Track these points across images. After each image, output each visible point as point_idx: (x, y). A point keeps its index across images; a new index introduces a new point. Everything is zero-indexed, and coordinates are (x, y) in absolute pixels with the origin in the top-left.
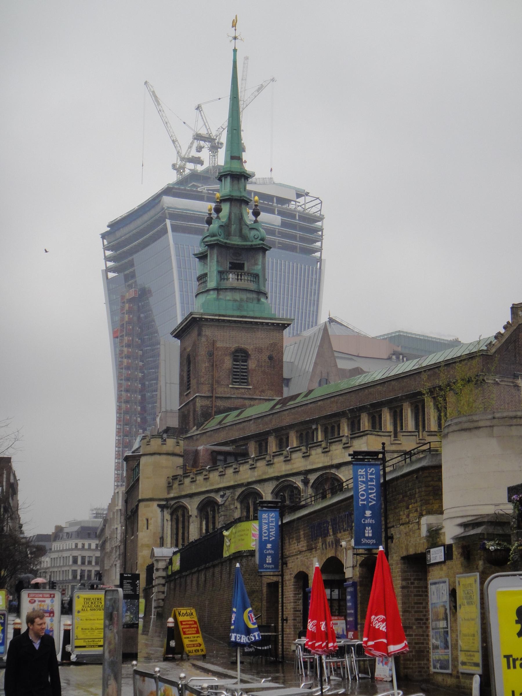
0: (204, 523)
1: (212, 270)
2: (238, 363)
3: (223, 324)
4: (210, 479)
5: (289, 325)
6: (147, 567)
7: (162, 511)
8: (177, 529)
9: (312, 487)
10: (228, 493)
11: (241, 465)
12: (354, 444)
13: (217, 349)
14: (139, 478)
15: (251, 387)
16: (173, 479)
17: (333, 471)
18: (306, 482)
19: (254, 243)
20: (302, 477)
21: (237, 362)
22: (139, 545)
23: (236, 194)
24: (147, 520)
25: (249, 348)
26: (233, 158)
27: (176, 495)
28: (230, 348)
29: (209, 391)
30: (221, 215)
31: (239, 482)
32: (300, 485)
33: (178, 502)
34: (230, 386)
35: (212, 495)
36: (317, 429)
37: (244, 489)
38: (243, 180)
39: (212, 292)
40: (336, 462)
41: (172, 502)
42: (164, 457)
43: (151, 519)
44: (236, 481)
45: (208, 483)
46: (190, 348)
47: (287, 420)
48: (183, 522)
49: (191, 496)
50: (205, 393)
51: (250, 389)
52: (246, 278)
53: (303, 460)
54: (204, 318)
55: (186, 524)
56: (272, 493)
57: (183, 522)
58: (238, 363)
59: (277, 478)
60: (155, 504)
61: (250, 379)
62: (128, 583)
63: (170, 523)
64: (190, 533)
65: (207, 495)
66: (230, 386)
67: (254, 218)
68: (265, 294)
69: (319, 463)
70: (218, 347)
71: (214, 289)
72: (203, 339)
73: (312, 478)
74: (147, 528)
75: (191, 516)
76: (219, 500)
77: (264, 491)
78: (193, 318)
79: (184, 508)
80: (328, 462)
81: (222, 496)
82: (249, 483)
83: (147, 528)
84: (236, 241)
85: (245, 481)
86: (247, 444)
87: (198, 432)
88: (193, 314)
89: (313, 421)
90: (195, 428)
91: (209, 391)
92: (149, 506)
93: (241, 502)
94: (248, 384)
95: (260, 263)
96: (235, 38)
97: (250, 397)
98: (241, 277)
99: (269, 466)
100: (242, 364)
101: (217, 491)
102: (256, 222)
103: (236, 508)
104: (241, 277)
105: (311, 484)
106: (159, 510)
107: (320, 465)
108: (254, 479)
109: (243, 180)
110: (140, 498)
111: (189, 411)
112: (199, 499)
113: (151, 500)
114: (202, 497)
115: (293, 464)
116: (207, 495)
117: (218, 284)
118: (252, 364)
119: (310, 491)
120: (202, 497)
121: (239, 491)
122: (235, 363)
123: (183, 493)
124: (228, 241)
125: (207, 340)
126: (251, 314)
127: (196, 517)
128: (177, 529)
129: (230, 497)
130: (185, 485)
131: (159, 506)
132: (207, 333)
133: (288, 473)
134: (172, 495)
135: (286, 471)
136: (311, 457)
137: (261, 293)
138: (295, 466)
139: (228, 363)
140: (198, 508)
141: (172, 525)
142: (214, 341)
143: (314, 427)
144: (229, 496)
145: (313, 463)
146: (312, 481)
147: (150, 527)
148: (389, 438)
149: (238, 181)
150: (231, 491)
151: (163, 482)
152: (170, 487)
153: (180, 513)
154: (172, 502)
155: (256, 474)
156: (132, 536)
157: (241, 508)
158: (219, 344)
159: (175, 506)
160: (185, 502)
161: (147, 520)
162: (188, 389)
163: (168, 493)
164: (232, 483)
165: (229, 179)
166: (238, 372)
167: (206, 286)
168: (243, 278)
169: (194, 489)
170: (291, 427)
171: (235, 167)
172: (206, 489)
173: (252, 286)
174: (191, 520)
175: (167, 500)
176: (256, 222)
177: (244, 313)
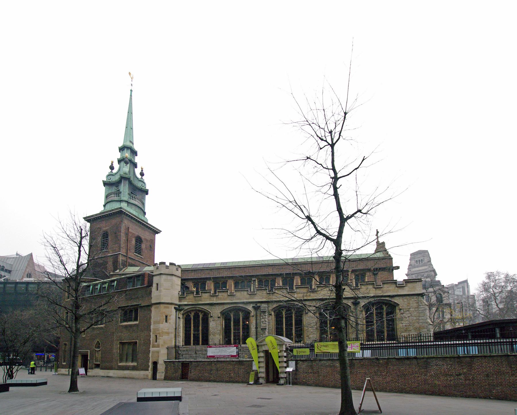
0: (224, 321)
10: (264, 305)
12: (408, 285)
18: (356, 304)
20: (352, 301)
24: (166, 317)
41: (186, 308)
43: (170, 316)
45: (235, 298)
50: (123, 253)
60: (173, 306)
63: (182, 320)
65: (235, 305)
74: (166, 321)
78: (121, 210)
83: (166, 321)
88: (122, 208)
92: (168, 308)
106: (174, 311)
112: (222, 307)
113: (171, 304)
116: (235, 305)
121: (275, 305)
131: (175, 308)
136: (361, 290)
141: (183, 321)
147: (169, 321)
153: (192, 315)
154: (186, 308)
155: (296, 296)
161: (166, 317)
168: (136, 200)
173: (141, 206)
175: (179, 306)
176: (142, 178)
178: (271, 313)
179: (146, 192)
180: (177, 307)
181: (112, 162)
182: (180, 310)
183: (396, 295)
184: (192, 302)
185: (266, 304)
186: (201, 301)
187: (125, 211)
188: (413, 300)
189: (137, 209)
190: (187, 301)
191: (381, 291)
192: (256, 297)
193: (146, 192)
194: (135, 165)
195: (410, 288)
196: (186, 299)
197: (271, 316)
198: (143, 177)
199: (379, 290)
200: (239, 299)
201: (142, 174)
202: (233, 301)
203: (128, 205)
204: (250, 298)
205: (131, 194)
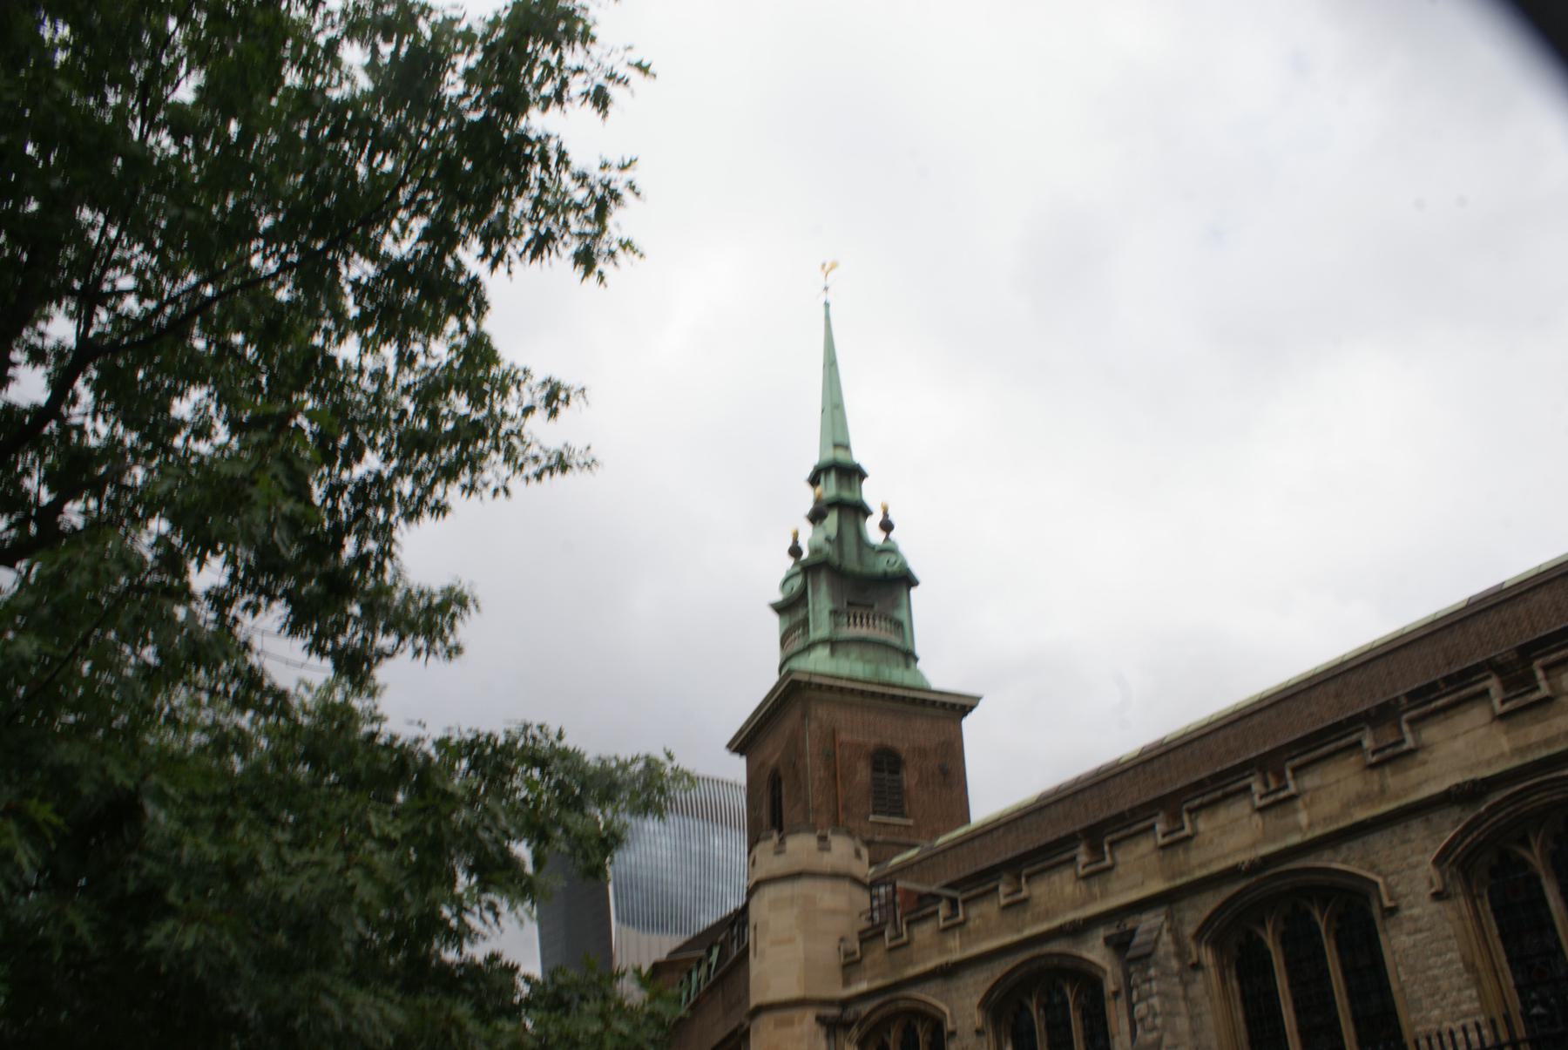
5: (972, 708)
10: (1149, 921)
15: (910, 822)
16: (862, 941)
23: (846, 495)
25: (902, 747)
26: (836, 446)
27: (878, 983)
31: (1199, 873)
33: (891, 1001)
34: (872, 818)
37: (1229, 891)
38: (857, 478)
41: (865, 1008)
42: (828, 884)
44: (1182, 874)
45: (1028, 916)
46: (777, 755)
49: (948, 972)
51: (907, 827)
56: (1438, 861)
60: (810, 1015)
66: (872, 818)
67: (882, 536)
68: (916, 659)
71: (823, 642)
72: (814, 725)
75: (953, 1034)
77: (1372, 867)
82: (1268, 860)
85: (1244, 858)
94: (902, 815)
99: (1388, 770)
101: (1077, 930)
103: (1197, 966)
108: (1295, 839)
109: (857, 478)
118: (909, 778)
121: (1209, 903)
123: (912, 971)
129: (1164, 932)
131: (820, 1020)
134: (863, 987)
137: (909, 657)
139: (863, 773)
140: (984, 1004)
144: (1162, 925)
151: (827, 951)
152: (850, 966)
154: (865, 1008)
155: (1303, 818)
158: (844, 736)
159: (874, 1018)
160: (928, 995)
163: (847, 982)
164: (1156, 886)
165: (833, 476)
168: (877, 622)
169: (957, 950)
173: (895, 640)
175: (845, 1003)
176: (887, 539)
178: (1194, 959)
179: (906, 580)
180: (833, 1012)
182: (847, 1026)
185: (1163, 910)
186: (911, 963)
189: (871, 653)
193: (906, 580)
194: (862, 511)
197: (1200, 976)
198: (893, 535)
200: (1048, 914)
201: (887, 526)
202: (1028, 932)
203: (833, 653)
204: (1091, 898)
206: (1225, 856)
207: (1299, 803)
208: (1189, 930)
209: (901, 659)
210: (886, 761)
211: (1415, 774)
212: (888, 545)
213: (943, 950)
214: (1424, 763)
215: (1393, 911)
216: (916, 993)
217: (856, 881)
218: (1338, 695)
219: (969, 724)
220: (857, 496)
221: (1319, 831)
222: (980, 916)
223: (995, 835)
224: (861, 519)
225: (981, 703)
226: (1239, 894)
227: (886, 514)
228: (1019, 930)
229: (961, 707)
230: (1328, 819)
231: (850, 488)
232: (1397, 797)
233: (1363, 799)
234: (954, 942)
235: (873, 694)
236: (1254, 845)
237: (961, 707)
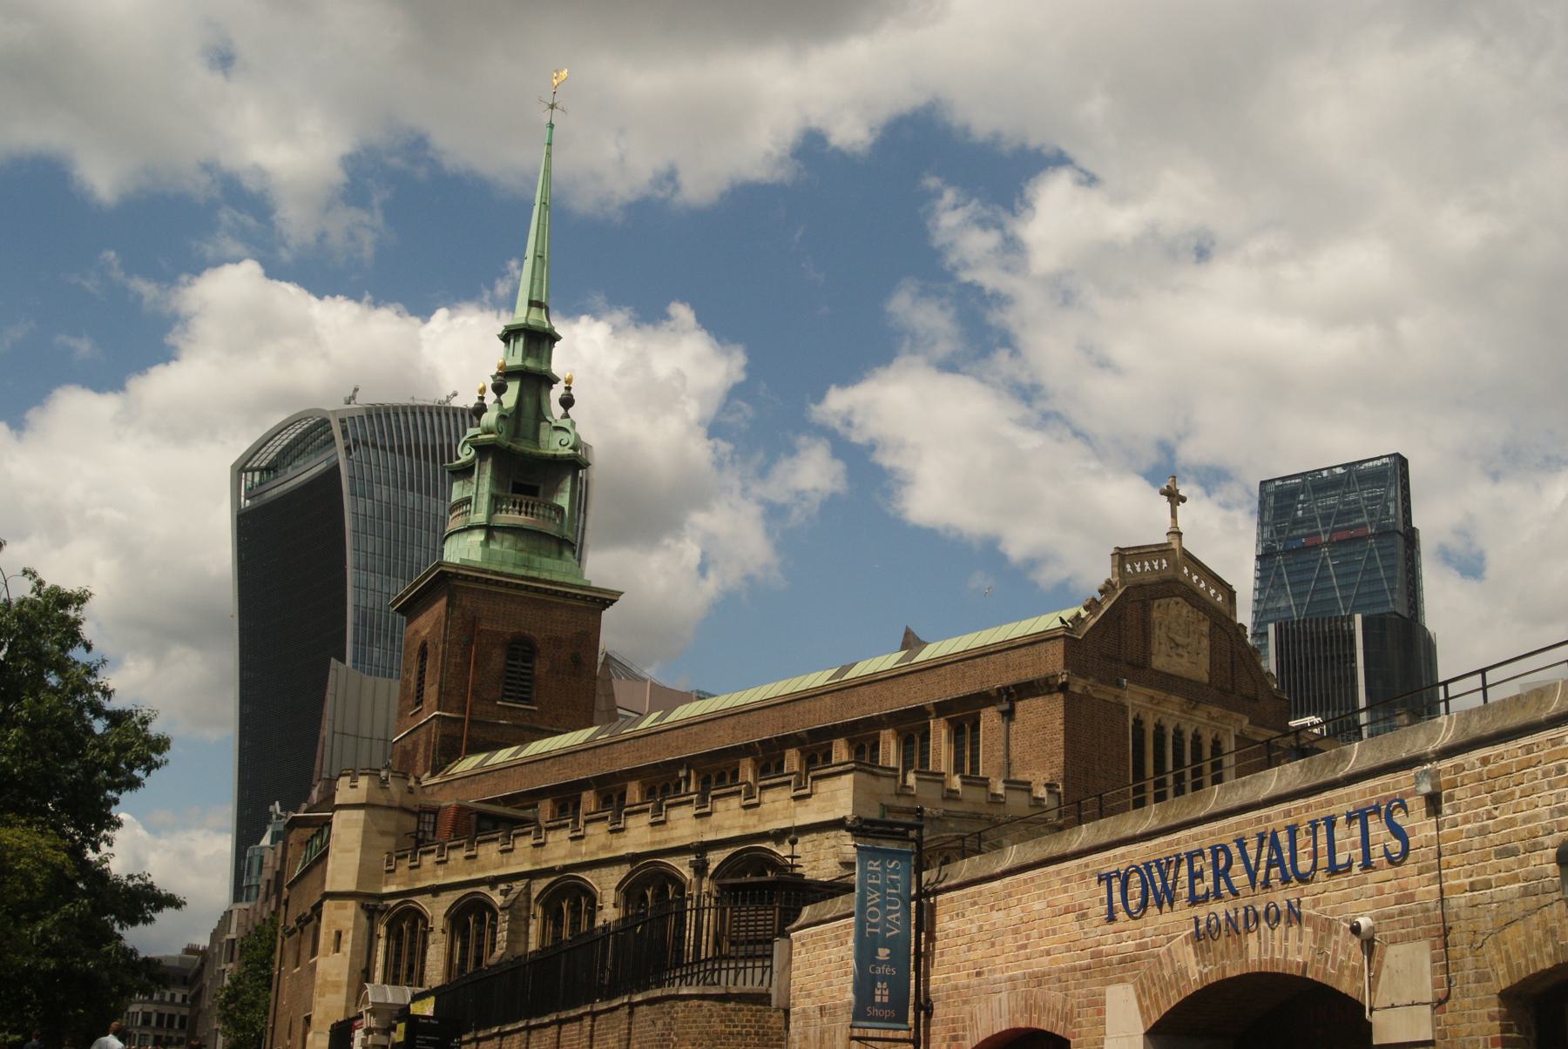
0: (458, 945)
1: (480, 491)
2: (515, 663)
3: (493, 589)
4: (479, 858)
5: (612, 602)
6: (332, 1026)
7: (371, 918)
8: (398, 955)
9: (712, 877)
11: (552, 832)
13: (478, 634)
14: (327, 850)
15: (536, 708)
17: (768, 845)
18: (700, 869)
19: (558, 453)
21: (513, 660)
22: (318, 981)
23: (530, 363)
27: (402, 888)
28: (504, 633)
29: (459, 708)
30: (503, 397)
31: (544, 866)
32: (687, 873)
34: (499, 703)
35: (484, 889)
36: (688, 779)
38: (547, 342)
39: (477, 531)
40: (770, 826)
44: (537, 864)
46: (428, 630)
47: (625, 762)
48: (412, 942)
49: (436, 891)
51: (534, 710)
52: (541, 512)
53: (694, 820)
54: (461, 575)
55: (419, 946)
56: (617, 889)
57: (412, 942)
58: (515, 663)
59: (632, 859)
61: (535, 694)
62: (429, 1043)
64: (428, 963)
66: (499, 703)
67: (562, 410)
69: (732, 828)
70: (482, 630)
71: (480, 527)
73: (715, 859)
76: (498, 899)
79: (418, 915)
80: (755, 826)
81: (505, 893)
82: (567, 868)
84: (525, 447)
85: (559, 863)
86: (536, 806)
87: (436, 780)
89: (678, 764)
90: (428, 774)
91: (459, 708)
93: (545, 906)
94: (529, 701)
95: (568, 489)
96: (552, 107)
97: (535, 725)
98: (533, 509)
99: (615, 835)
100: (523, 664)
101: (493, 882)
102: (566, 416)
104: (533, 509)
105: (710, 872)
107: (736, 833)
108: (578, 860)
109: (547, 342)
110: (327, 889)
111: (415, 744)
112: (450, 897)
114: (459, 894)
115: (672, 829)
117: (490, 516)
118: (541, 667)
119: (706, 885)
120: (459, 894)
121: (545, 882)
122: (510, 662)
123: (419, 885)
124: (514, 445)
125: (463, 615)
126: (545, 576)
127: (443, 932)
128: (398, 955)
130: (422, 868)
132: (464, 603)
133: (657, 847)
135: (653, 843)
138: (675, 833)
139: (498, 660)
141: (387, 947)
142: (475, 618)
143: (682, 773)
145: (719, 828)
146: (713, 866)
148: (893, 781)
149: (539, 344)
150: (525, 881)
154: (392, 903)
155: (584, 849)
156: (297, 967)
157: (544, 917)
158: (484, 626)
162: (417, 705)
164: (527, 867)
166: (515, 678)
167: (469, 520)
168: (535, 511)
170: (633, 774)
171: (536, 318)
172: (468, 878)
173: (552, 529)
174: (431, 937)
177: (534, 574)
181: (483, 390)
183: (782, 830)
184: (404, 884)
186: (419, 880)
187: (454, 570)
188: (827, 843)
190: (398, 880)
191: (756, 817)
192: (512, 861)
194: (550, 380)
195: (824, 801)
196: (396, 877)
198: (570, 411)
199: (753, 814)
200: (483, 869)
201: (567, 402)
205: (515, 495)
206: (555, 859)
207: (584, 841)
208: (534, 895)
209: (554, 547)
210: (521, 649)
211: (622, 840)
212: (566, 423)
213: (437, 877)
214: (625, 837)
215: (601, 908)
216: (416, 899)
217: (404, 810)
218: (734, 728)
219: (607, 614)
220: (544, 368)
221: (587, 859)
222: (455, 859)
223: (548, 763)
224: (544, 389)
225: (621, 598)
226: (550, 885)
227: (568, 389)
228: (470, 874)
229: (604, 600)
230: (592, 853)
231: (538, 357)
232: (614, 851)
233: (604, 848)
234: (440, 871)
235: (517, 586)
236: (565, 857)
237: (604, 600)
